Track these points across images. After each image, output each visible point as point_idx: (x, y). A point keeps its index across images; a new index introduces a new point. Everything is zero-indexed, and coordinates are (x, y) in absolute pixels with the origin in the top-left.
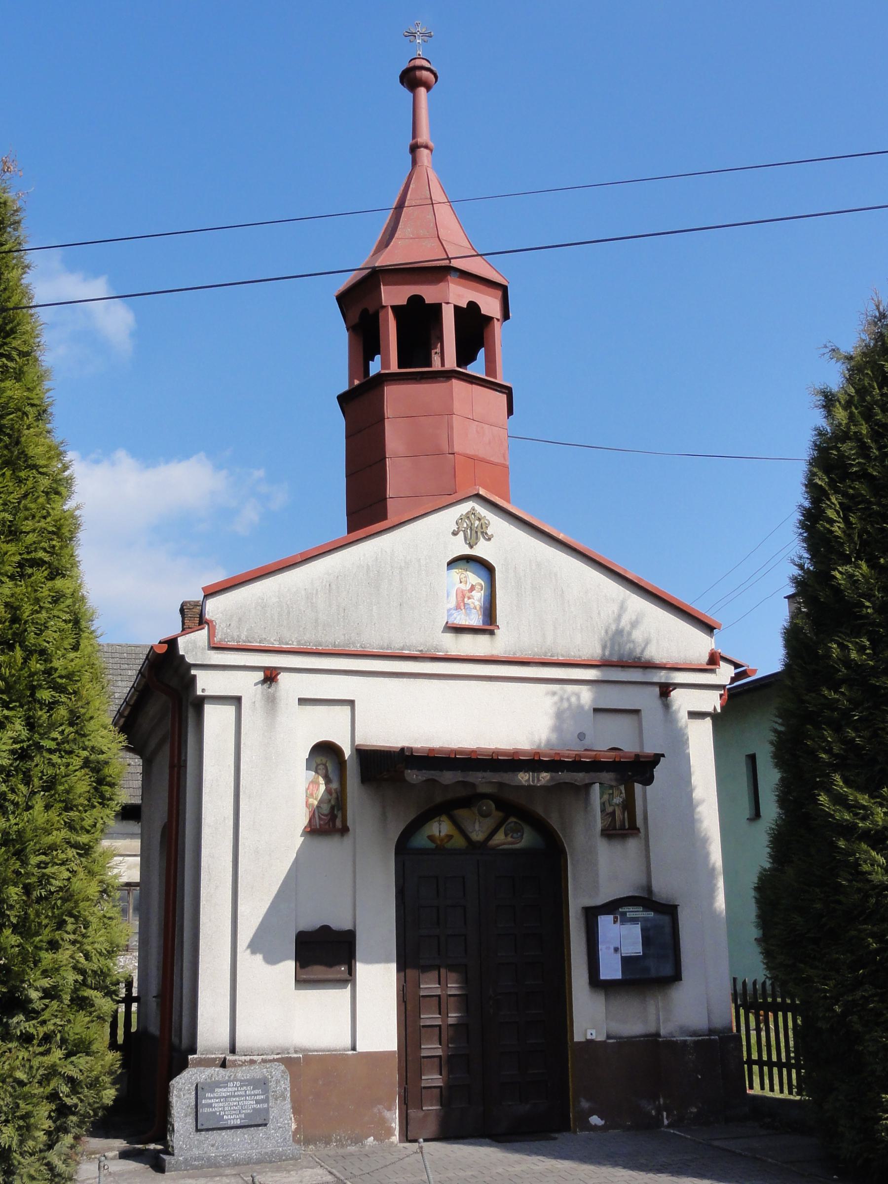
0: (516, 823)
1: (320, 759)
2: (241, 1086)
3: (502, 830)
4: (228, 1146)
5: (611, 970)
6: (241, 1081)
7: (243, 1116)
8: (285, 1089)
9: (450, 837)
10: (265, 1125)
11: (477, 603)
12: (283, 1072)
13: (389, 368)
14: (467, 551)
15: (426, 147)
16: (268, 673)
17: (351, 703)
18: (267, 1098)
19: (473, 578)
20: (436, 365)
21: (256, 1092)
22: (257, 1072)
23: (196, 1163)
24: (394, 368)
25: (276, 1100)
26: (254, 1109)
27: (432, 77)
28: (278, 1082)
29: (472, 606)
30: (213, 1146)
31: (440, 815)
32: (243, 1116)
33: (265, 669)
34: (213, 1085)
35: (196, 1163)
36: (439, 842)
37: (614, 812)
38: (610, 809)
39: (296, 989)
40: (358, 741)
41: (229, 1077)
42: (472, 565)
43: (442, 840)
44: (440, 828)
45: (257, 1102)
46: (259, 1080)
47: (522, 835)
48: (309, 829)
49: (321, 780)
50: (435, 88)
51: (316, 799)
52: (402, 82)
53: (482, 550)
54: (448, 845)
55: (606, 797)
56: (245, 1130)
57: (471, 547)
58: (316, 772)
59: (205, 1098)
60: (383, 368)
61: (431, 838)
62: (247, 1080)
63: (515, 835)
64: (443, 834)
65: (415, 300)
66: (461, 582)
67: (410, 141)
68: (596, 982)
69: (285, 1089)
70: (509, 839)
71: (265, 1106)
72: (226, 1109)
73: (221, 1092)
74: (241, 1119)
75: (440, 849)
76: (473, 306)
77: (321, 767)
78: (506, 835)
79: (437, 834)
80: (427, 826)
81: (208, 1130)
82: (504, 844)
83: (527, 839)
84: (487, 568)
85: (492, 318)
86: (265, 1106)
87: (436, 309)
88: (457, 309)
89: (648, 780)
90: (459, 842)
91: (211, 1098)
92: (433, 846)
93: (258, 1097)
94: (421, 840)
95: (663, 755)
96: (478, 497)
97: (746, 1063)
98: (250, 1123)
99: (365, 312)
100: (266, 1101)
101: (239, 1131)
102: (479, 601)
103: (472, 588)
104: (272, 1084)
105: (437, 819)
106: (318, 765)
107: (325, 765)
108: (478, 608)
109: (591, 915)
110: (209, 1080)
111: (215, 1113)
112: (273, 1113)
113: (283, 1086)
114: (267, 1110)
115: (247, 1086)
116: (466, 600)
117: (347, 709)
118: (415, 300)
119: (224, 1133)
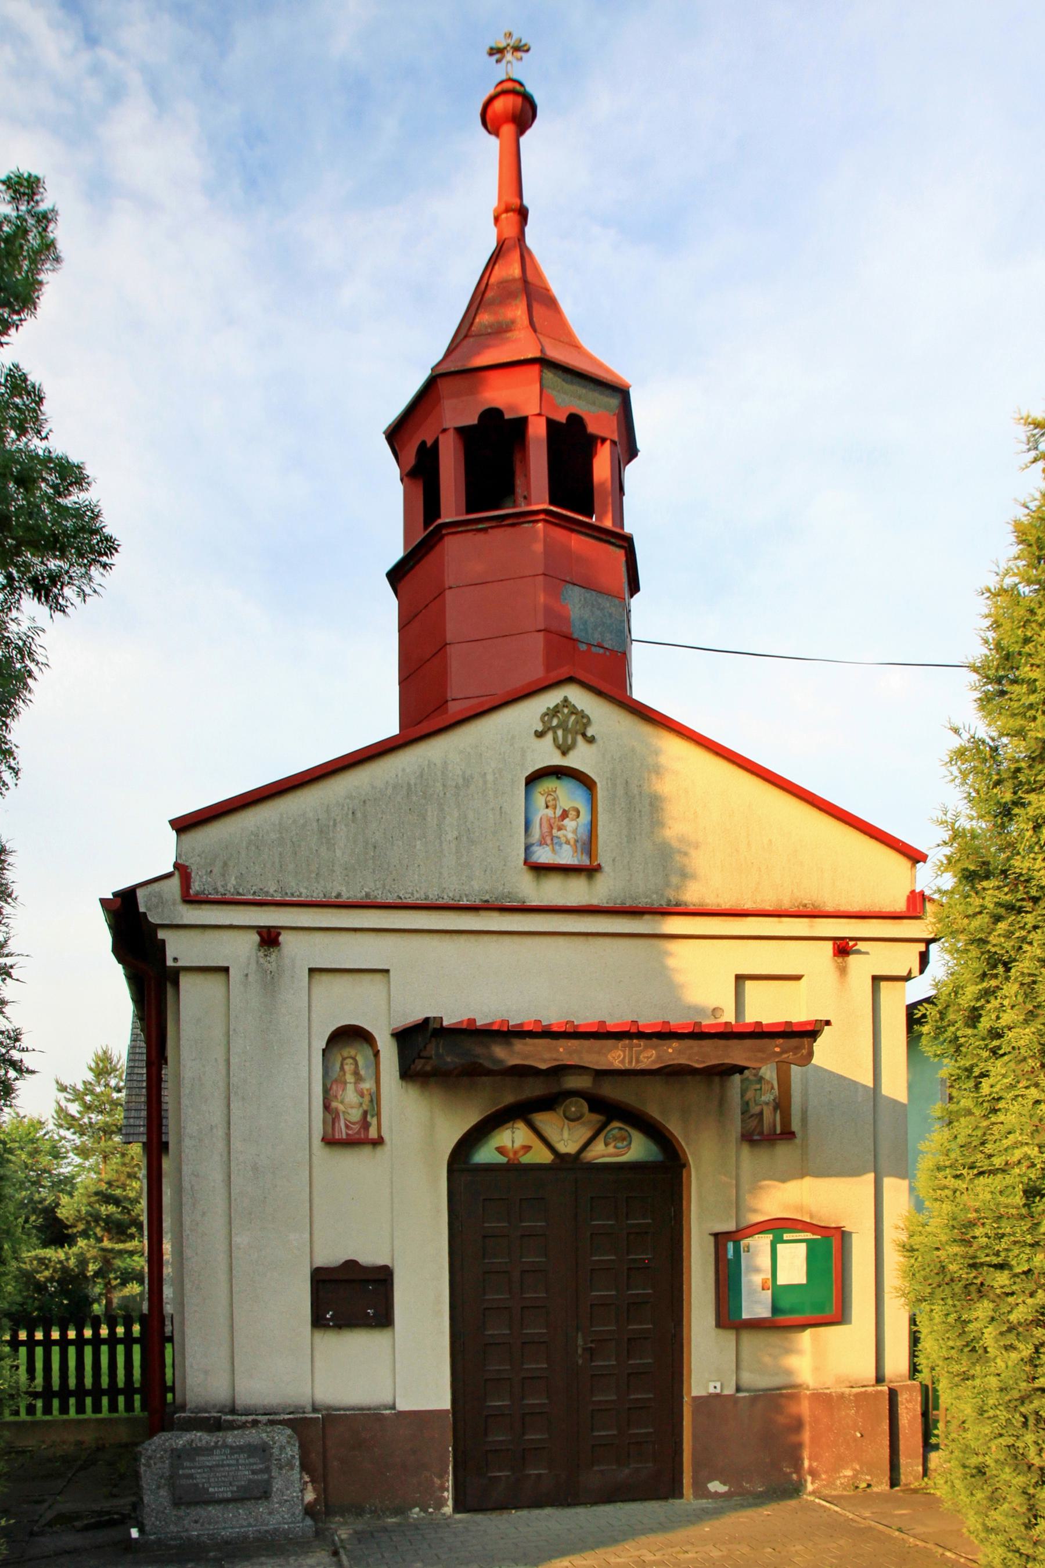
0: (621, 1129)
2: (232, 1454)
4: (217, 1522)
6: (231, 1448)
7: (235, 1489)
9: (527, 1148)
21: (252, 1460)
25: (281, 1468)
26: (250, 1481)
28: (282, 1448)
30: (196, 1522)
32: (235, 1489)
36: (511, 1155)
37: (761, 1113)
41: (216, 1443)
43: (515, 1153)
45: (254, 1472)
47: (630, 1143)
59: (183, 1468)
61: (501, 1150)
63: (620, 1145)
70: (611, 1149)
71: (266, 1476)
72: (212, 1480)
73: (203, 1460)
74: (232, 1492)
78: (606, 1144)
79: (509, 1145)
82: (603, 1156)
86: (266, 1476)
91: (191, 1468)
92: (503, 1160)
94: (486, 1154)
100: (267, 1470)
111: (196, 1485)
113: (290, 1453)
115: (239, 1453)
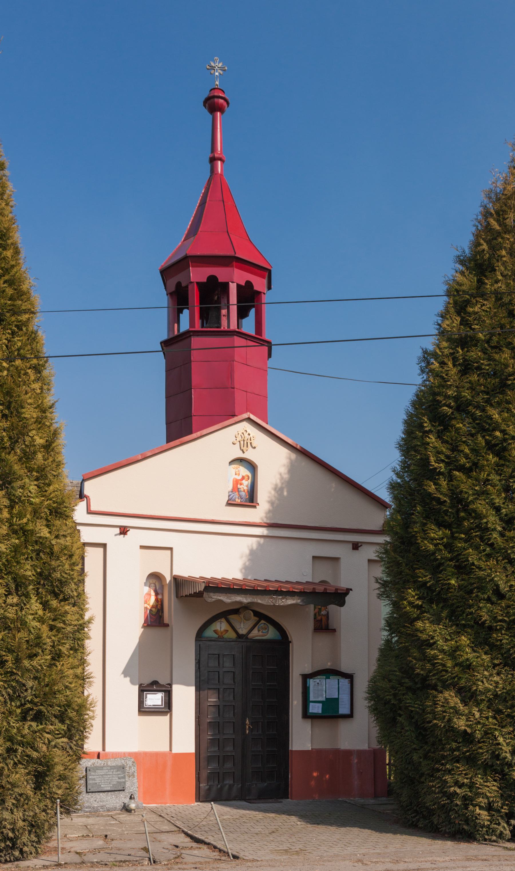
0: (265, 624)
1: (151, 581)
2: (111, 769)
3: (256, 628)
4: (103, 801)
5: (315, 709)
6: (110, 767)
7: (111, 785)
8: (134, 771)
9: (227, 631)
10: (124, 790)
11: (245, 488)
12: (133, 762)
13: (195, 328)
14: (241, 455)
15: (220, 159)
16: (122, 529)
17: (171, 549)
18: (125, 776)
19: (244, 471)
20: (224, 326)
21: (119, 773)
22: (119, 762)
23: (87, 810)
24: (198, 327)
25: (129, 777)
26: (118, 782)
27: (225, 104)
28: (130, 767)
29: (242, 490)
30: (95, 801)
31: (221, 618)
32: (111, 785)
33: (120, 527)
34: (96, 768)
35: (87, 810)
36: (220, 634)
37: (321, 619)
38: (319, 618)
39: (139, 715)
40: (175, 573)
41: (104, 764)
42: (243, 463)
43: (222, 633)
44: (221, 626)
45: (119, 778)
46: (120, 766)
47: (268, 631)
48: (146, 625)
49: (153, 593)
50: (227, 109)
51: (149, 605)
52: (205, 105)
53: (249, 455)
54: (226, 636)
55: (317, 610)
56: (112, 793)
57: (244, 452)
58: (150, 587)
59: (91, 775)
60: (190, 327)
61: (215, 631)
62: (114, 766)
63: (264, 631)
64: (222, 629)
65: (212, 279)
66: (236, 474)
67: (209, 155)
68: (306, 715)
69: (134, 771)
70: (260, 633)
71: (124, 780)
72: (102, 781)
73: (99, 772)
74: (111, 787)
75: (220, 638)
76: (249, 284)
77: (153, 585)
78: (259, 631)
79: (219, 629)
80: (214, 624)
81: (92, 792)
82: (257, 636)
83: (271, 634)
84: (252, 466)
85: (261, 292)
86: (124, 780)
87: (225, 287)
88: (238, 286)
89: (342, 603)
90: (232, 635)
91: (94, 775)
93: (119, 776)
94: (209, 633)
95: (351, 590)
96: (249, 420)
97: (387, 765)
98: (116, 789)
99: (179, 284)
100: (124, 777)
101: (110, 793)
102: (247, 486)
103: (243, 478)
104: (127, 769)
105: (220, 620)
106: (150, 584)
107: (155, 584)
108: (246, 491)
109: (305, 678)
110: (93, 766)
111: (96, 783)
112: (128, 784)
113: (133, 770)
114: (125, 783)
116: (239, 485)
117: (169, 552)
118: (212, 279)
119: (101, 794)
